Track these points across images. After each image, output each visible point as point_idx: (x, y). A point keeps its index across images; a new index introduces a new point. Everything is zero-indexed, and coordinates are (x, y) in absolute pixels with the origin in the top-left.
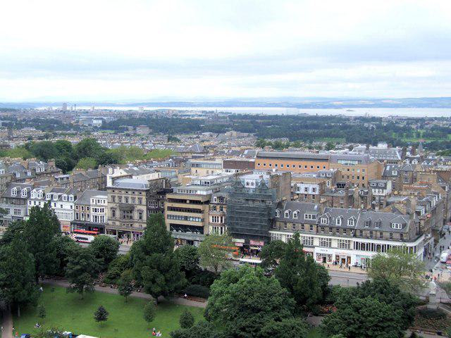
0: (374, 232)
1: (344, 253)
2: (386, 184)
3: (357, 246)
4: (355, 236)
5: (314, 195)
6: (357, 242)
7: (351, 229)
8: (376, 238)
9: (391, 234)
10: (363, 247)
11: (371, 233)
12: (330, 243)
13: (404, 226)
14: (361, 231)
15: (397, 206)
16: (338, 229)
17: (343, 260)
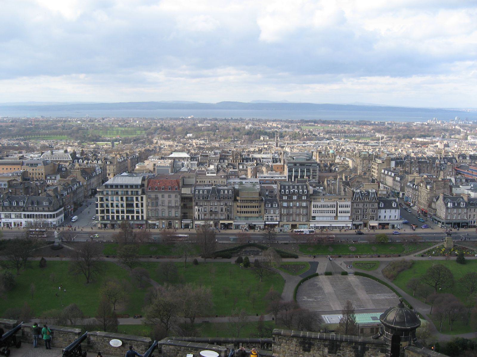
0: (34, 208)
1: (18, 220)
2: (55, 177)
3: (25, 216)
4: (24, 211)
5: (5, 188)
6: (25, 214)
7: (22, 207)
8: (36, 211)
9: (43, 209)
10: (29, 216)
11: (33, 208)
12: (10, 216)
13: (50, 203)
14: (27, 208)
15: (48, 192)
16: (14, 207)
17: (18, 225)
